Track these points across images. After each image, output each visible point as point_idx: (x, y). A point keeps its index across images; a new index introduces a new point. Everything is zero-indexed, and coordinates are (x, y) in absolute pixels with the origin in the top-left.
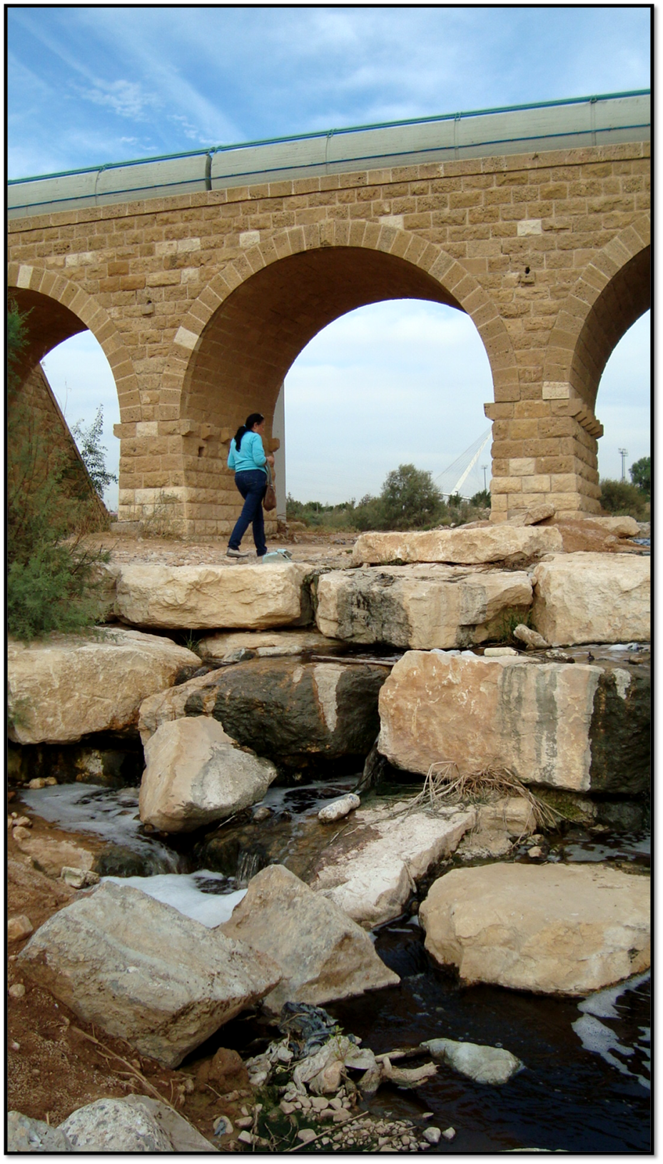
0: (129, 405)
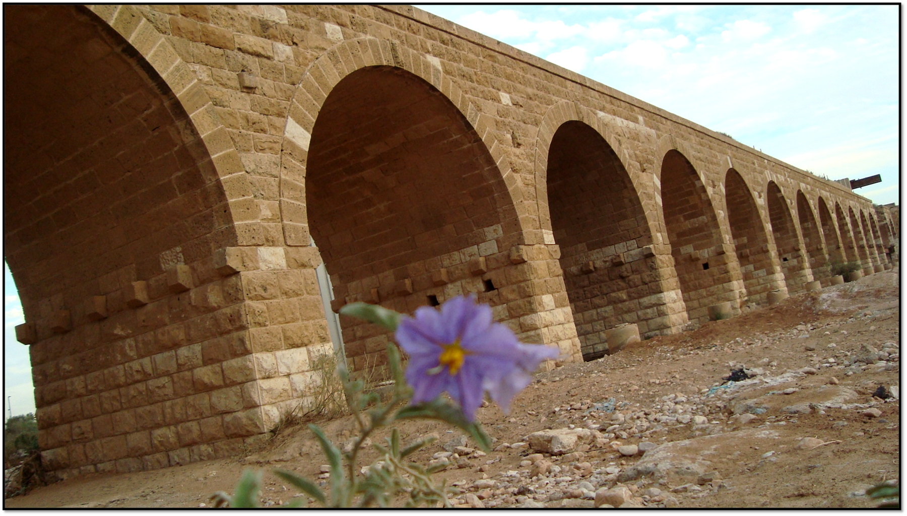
0: (246, 219)
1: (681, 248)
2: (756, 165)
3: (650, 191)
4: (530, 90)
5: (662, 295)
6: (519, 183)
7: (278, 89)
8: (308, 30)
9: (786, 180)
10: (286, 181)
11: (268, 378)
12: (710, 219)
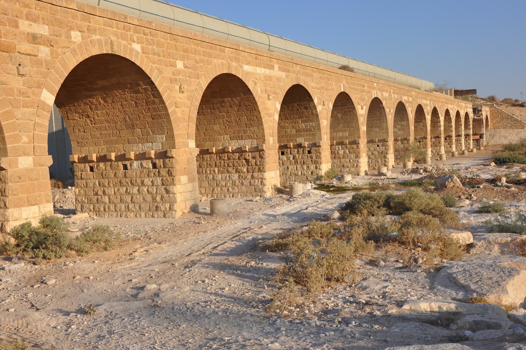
1: (297, 139)
2: (366, 87)
3: (271, 111)
4: (198, 57)
5: (265, 174)
6: (179, 114)
7: (39, 73)
8: (61, 37)
9: (390, 95)
10: (38, 122)
11: (16, 220)
12: (316, 125)
